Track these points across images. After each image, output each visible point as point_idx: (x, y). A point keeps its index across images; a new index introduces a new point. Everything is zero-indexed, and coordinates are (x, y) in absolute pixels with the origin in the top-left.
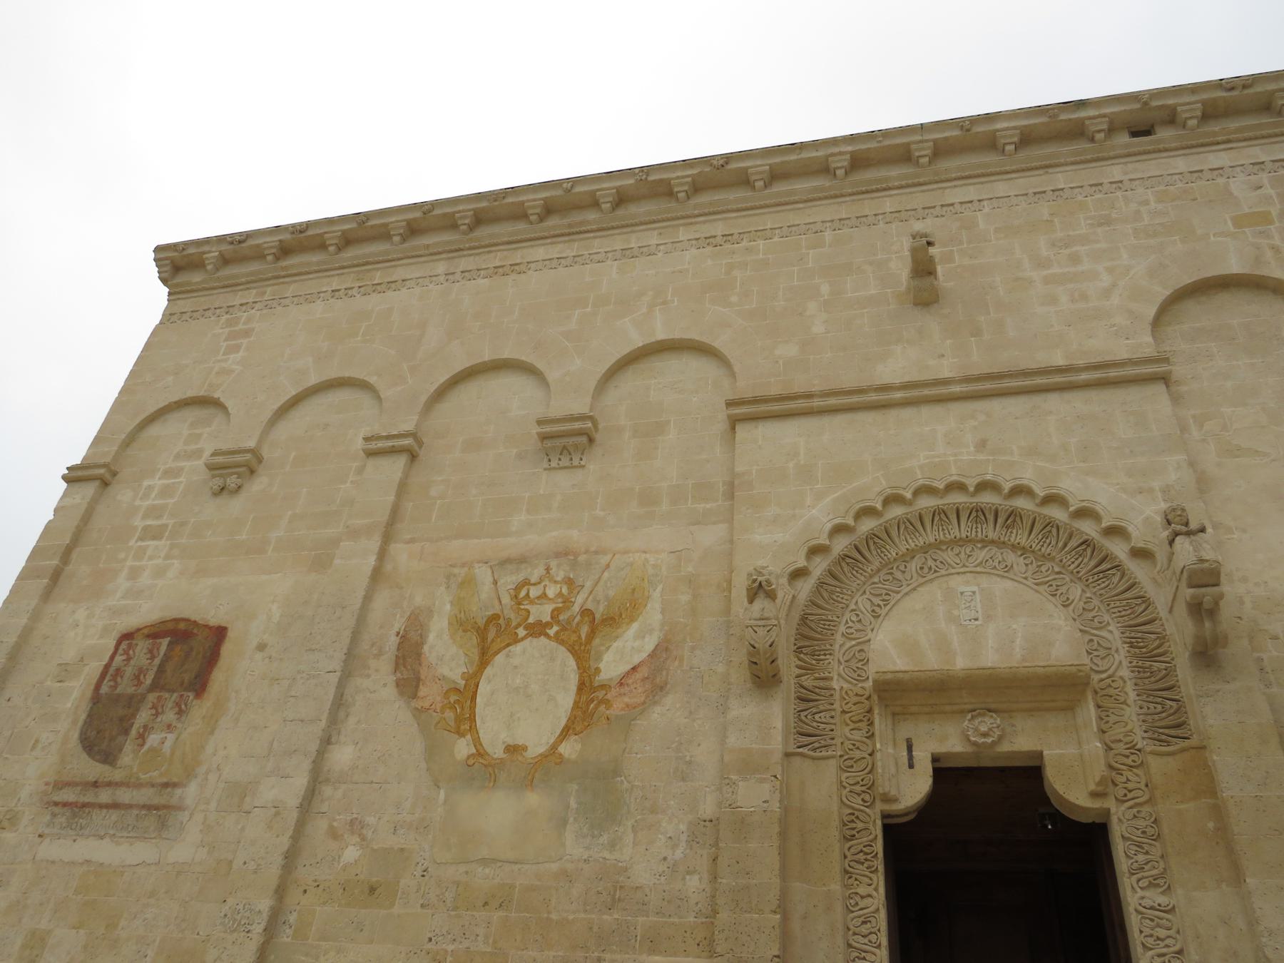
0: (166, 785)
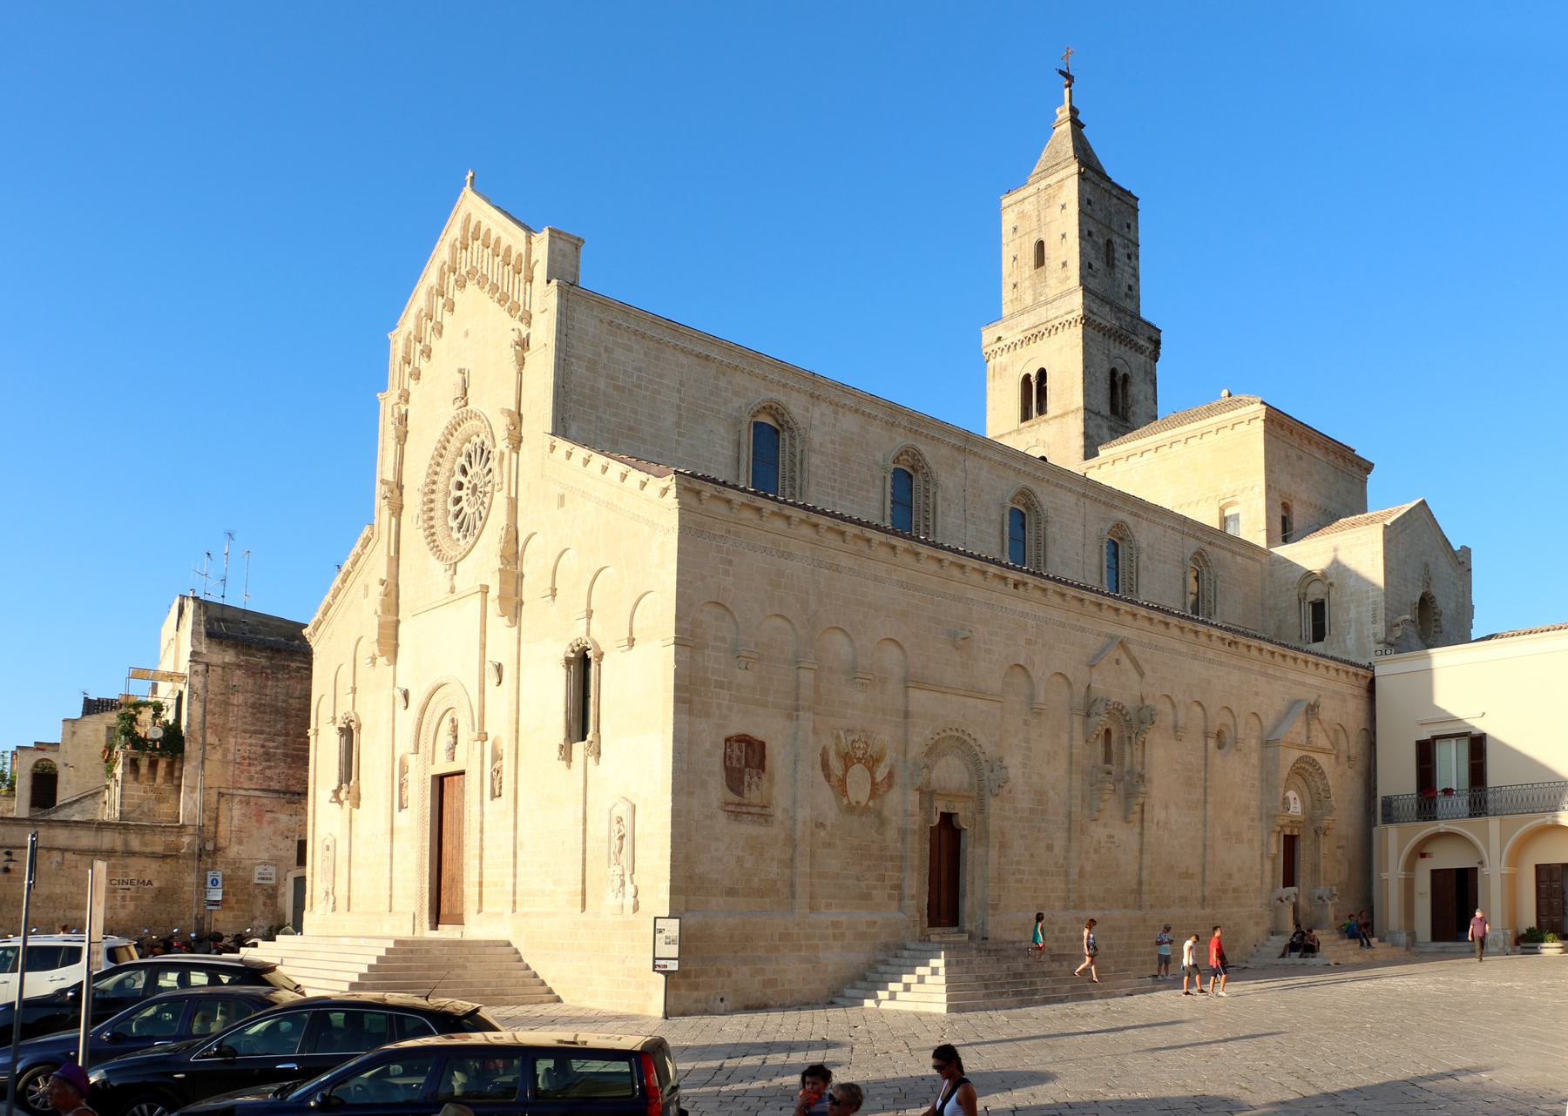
0: (764, 807)
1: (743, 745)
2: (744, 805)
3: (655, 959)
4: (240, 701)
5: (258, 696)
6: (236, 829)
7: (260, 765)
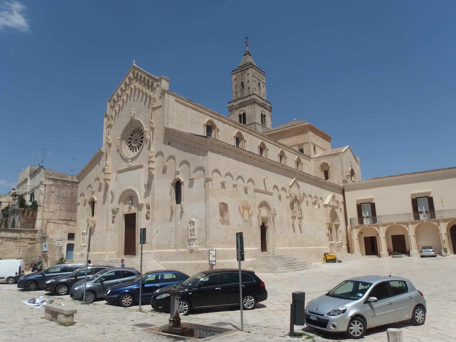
0: (228, 221)
1: (223, 205)
2: (224, 220)
3: (209, 261)
4: (54, 195)
5: (58, 193)
6: (51, 230)
7: (59, 212)
